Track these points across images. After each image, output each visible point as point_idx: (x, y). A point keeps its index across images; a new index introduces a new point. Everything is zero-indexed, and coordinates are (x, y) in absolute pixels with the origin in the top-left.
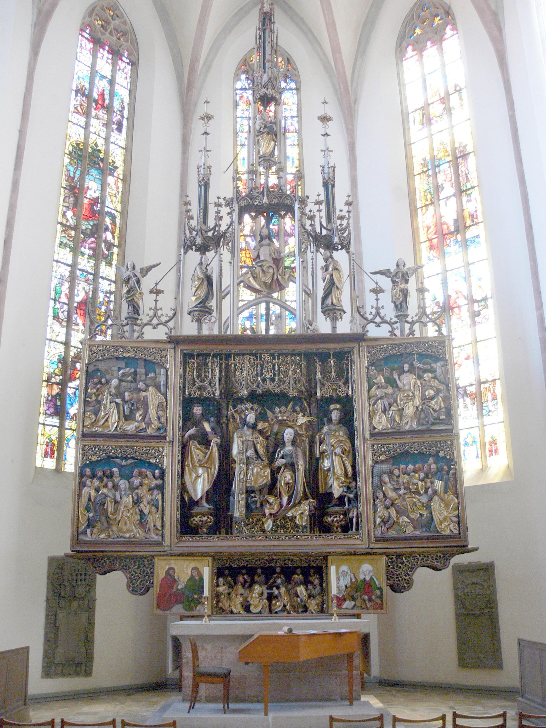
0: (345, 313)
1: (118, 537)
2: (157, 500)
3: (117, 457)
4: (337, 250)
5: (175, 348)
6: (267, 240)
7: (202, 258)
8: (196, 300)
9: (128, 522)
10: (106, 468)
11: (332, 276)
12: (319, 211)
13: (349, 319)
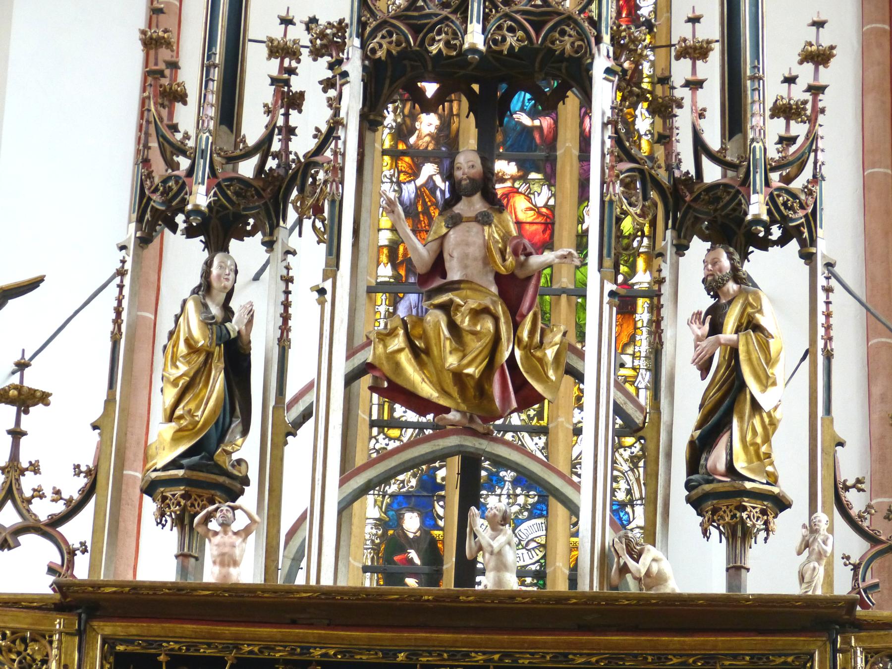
0: (781, 504)
4: (764, 244)
5: (80, 633)
6: (477, 198)
7: (208, 264)
8: (177, 439)
11: (734, 352)
12: (695, 85)
13: (798, 535)
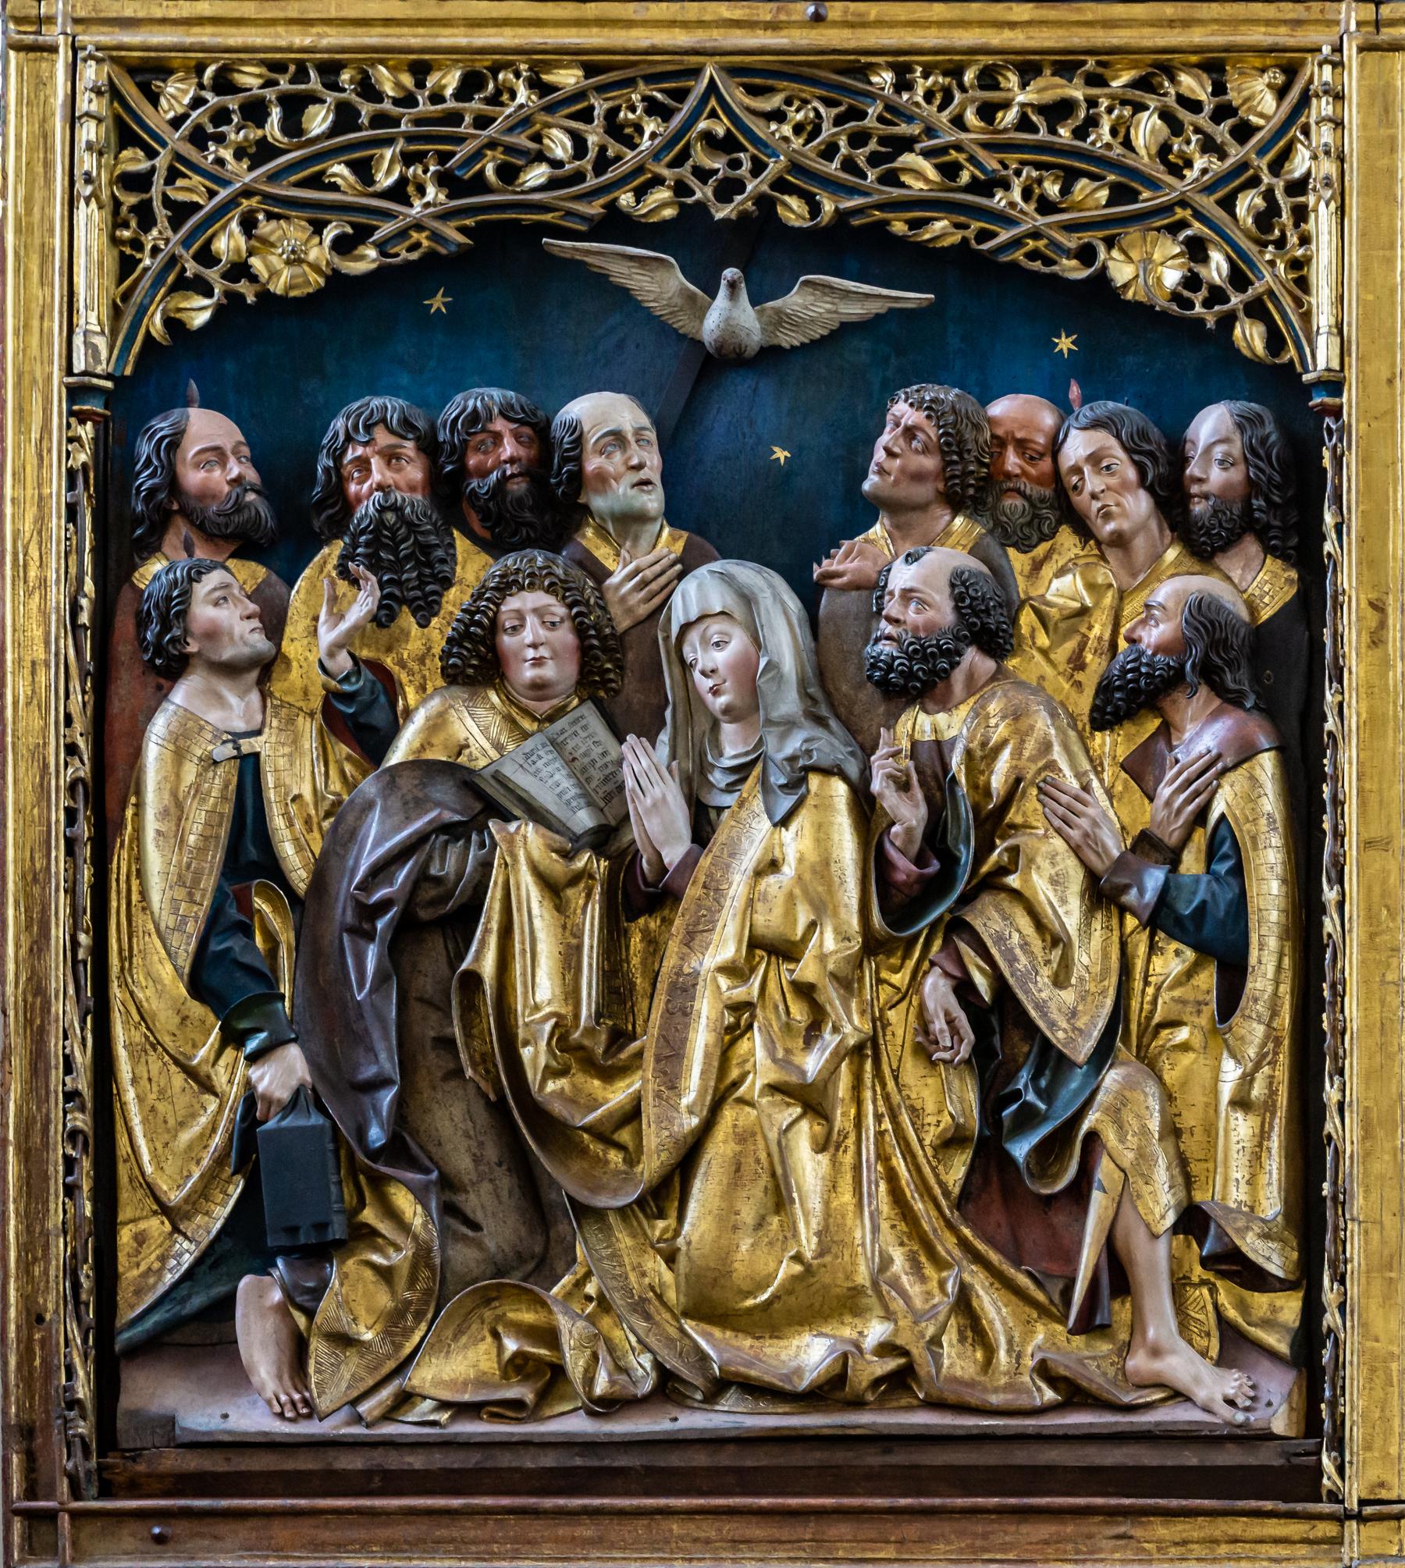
1: (668, 1388)
2: (1226, 848)
3: (616, 226)
9: (809, 1168)
10: (471, 399)
